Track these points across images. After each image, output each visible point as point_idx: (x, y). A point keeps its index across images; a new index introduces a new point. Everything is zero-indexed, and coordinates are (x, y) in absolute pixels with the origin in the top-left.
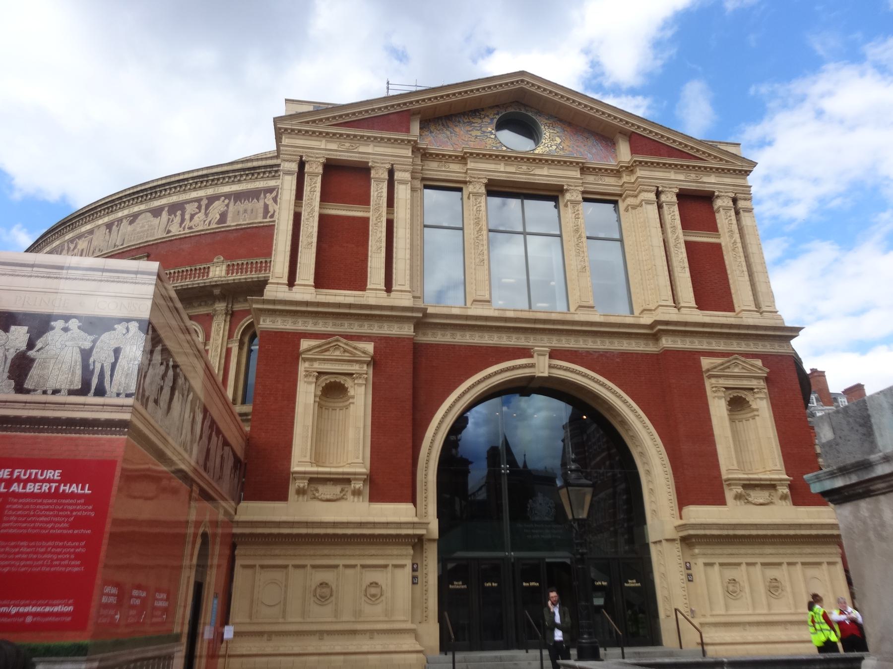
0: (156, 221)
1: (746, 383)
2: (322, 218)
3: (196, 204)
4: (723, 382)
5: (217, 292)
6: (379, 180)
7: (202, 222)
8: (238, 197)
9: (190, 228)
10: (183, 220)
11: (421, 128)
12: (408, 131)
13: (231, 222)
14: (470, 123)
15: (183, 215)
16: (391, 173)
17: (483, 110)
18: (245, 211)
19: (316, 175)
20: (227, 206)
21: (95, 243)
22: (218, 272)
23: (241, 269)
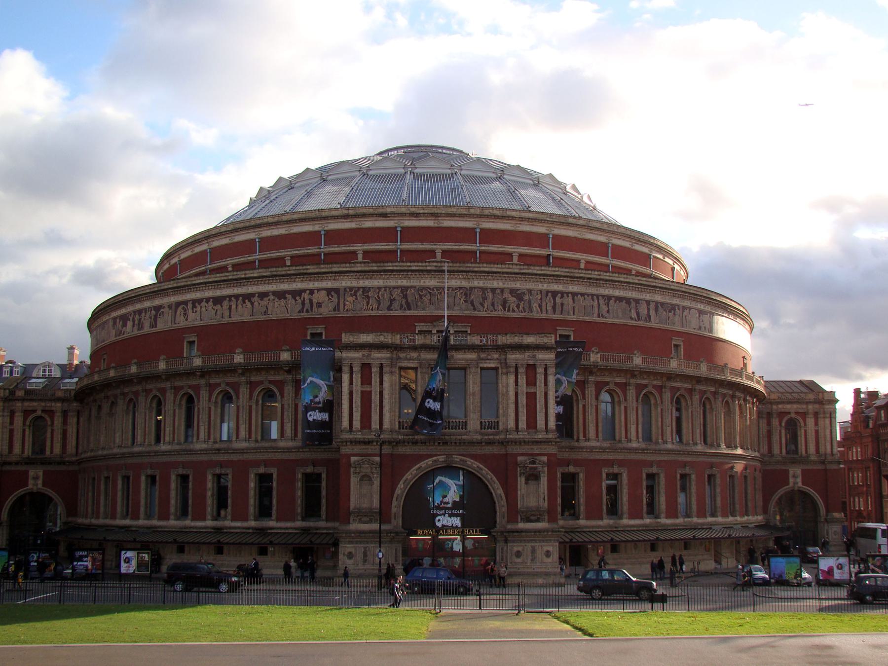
22: (285, 356)
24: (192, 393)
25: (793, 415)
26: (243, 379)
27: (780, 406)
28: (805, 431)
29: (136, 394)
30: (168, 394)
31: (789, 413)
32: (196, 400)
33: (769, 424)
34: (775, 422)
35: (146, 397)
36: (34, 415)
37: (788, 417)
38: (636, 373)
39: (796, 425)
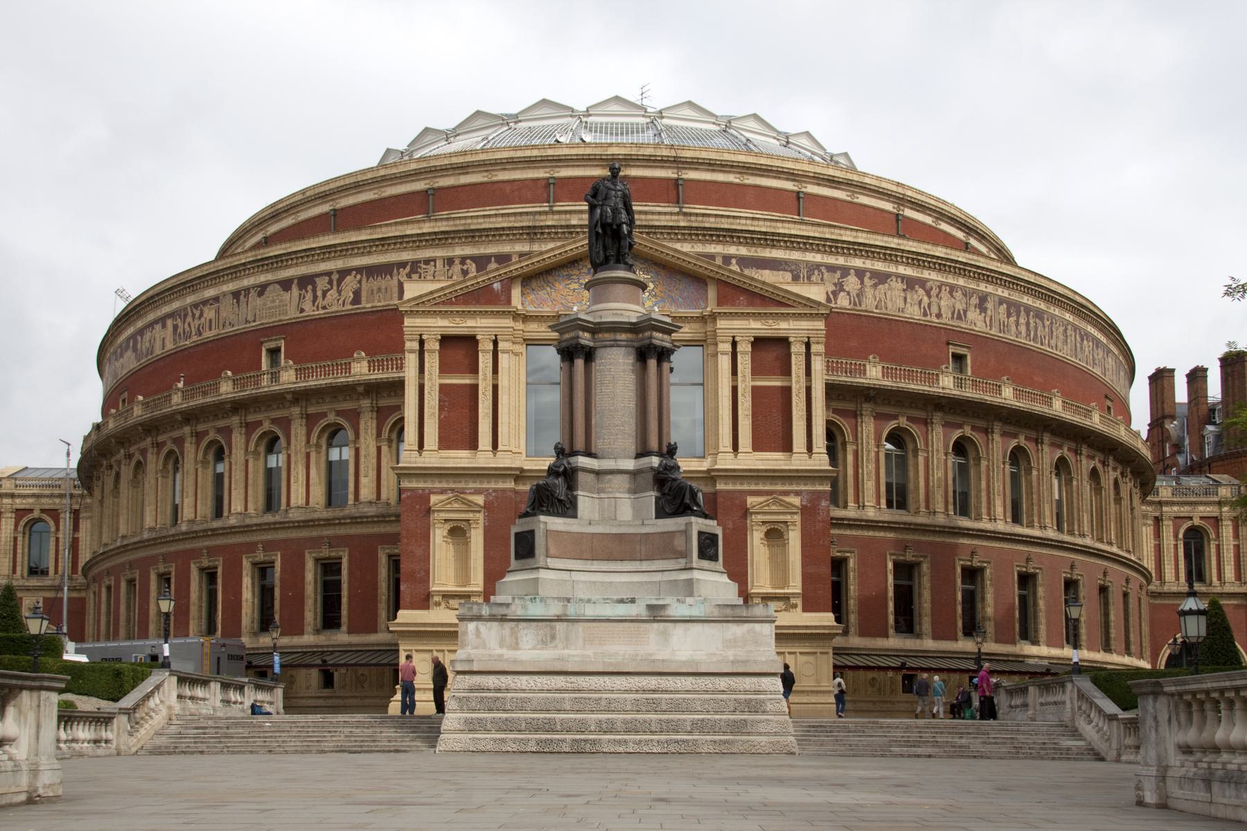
0: (287, 296)
1: (781, 518)
2: (442, 387)
3: (327, 278)
4: (761, 518)
5: (360, 389)
6: (485, 351)
7: (336, 302)
8: (372, 271)
9: (324, 308)
10: (315, 298)
11: (523, 294)
12: (509, 302)
13: (366, 305)
14: (569, 277)
15: (314, 291)
16: (495, 343)
17: (581, 260)
18: (379, 290)
19: (434, 351)
20: (360, 282)
21: (223, 314)
23: (381, 366)
24: (219, 438)
25: (1197, 522)
26: (296, 411)
27: (1175, 508)
28: (1218, 547)
29: (143, 452)
30: (187, 445)
31: (1191, 518)
32: (227, 452)
33: (1158, 534)
34: (1168, 530)
35: (158, 454)
36: (30, 516)
37: (1189, 523)
38: (944, 401)
39: (1202, 538)
